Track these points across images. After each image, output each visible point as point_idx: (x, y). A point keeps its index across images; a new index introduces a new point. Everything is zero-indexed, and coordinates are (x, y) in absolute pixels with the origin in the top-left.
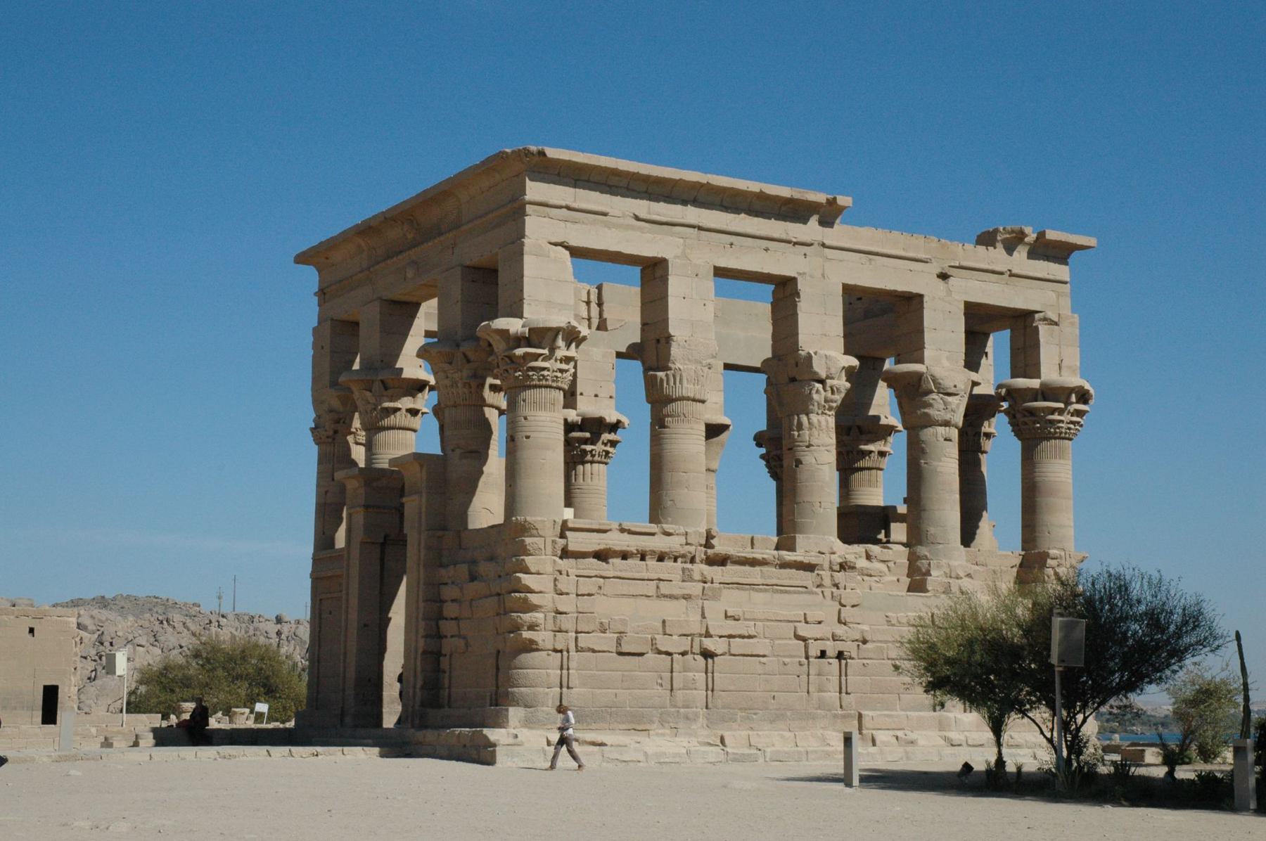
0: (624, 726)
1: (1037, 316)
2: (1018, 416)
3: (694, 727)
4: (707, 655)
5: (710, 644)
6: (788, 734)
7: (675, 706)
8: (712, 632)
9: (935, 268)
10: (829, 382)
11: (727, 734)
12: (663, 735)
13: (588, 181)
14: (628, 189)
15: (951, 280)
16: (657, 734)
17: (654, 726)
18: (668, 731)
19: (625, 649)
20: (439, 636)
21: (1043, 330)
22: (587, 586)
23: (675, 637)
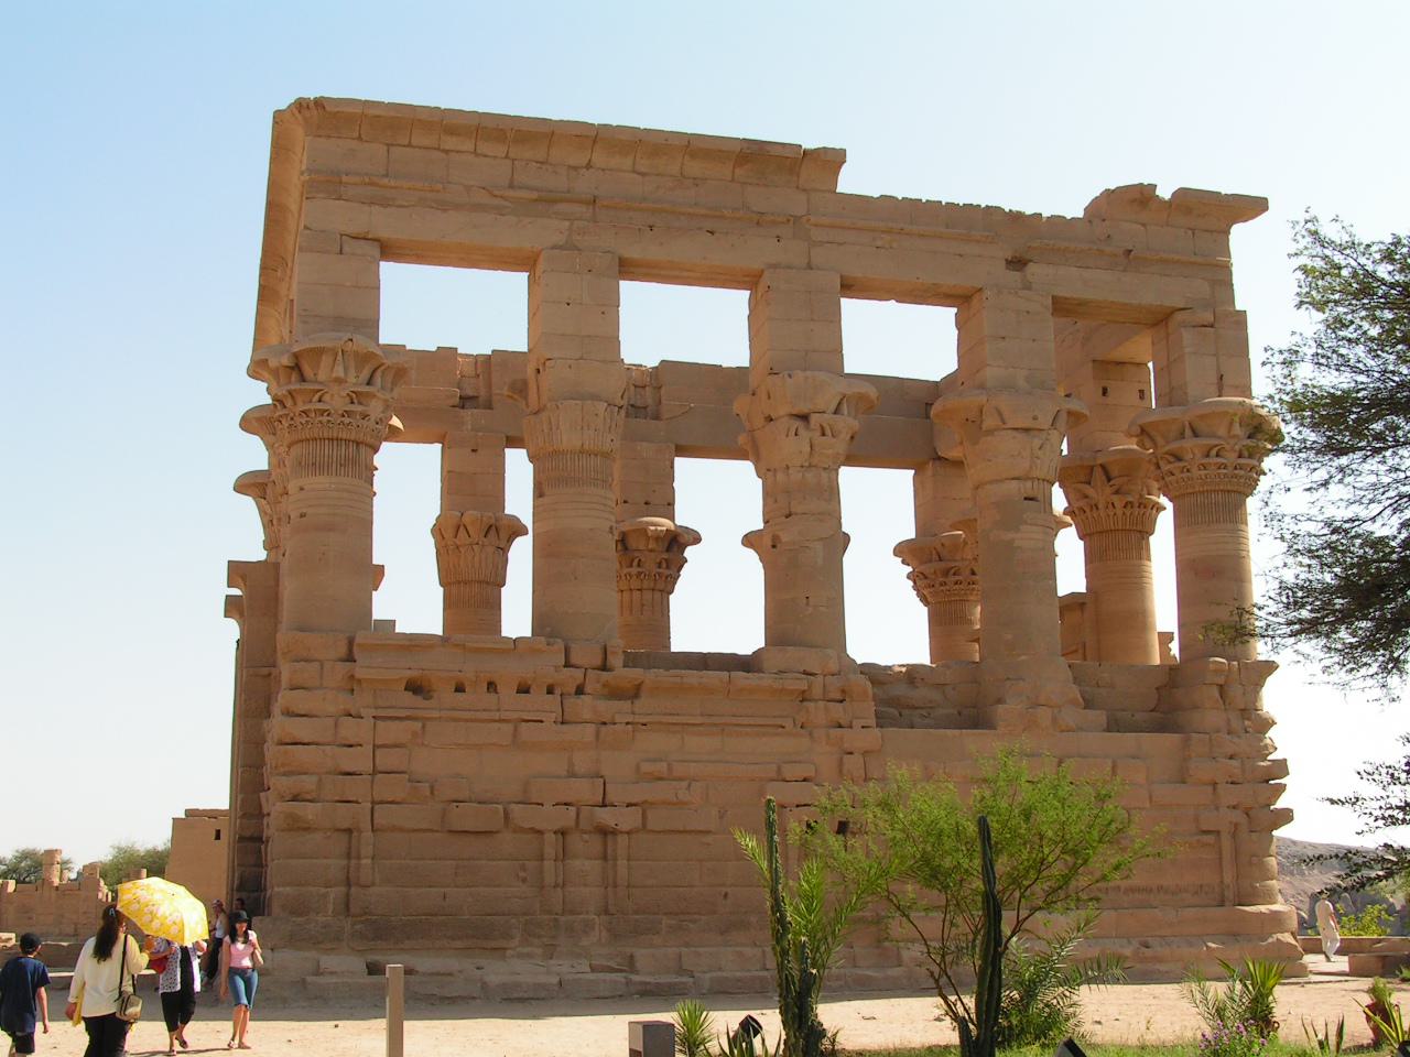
0: (459, 944)
1: (1179, 316)
2: (1161, 463)
3: (585, 942)
4: (605, 832)
5: (606, 817)
6: (748, 951)
7: (549, 912)
8: (611, 797)
9: (1004, 252)
10: (814, 418)
11: (642, 955)
12: (529, 956)
13: (409, 145)
14: (475, 152)
15: (1032, 268)
16: (520, 956)
17: (516, 941)
18: (539, 951)
19: (454, 829)
20: (260, 815)
21: (1188, 336)
22: (393, 731)
23: (548, 807)
